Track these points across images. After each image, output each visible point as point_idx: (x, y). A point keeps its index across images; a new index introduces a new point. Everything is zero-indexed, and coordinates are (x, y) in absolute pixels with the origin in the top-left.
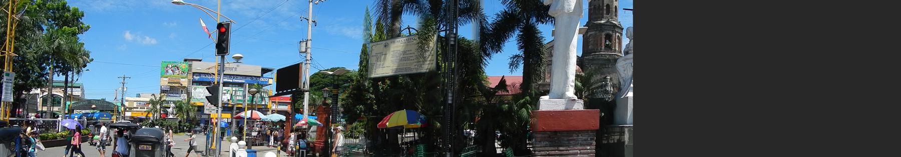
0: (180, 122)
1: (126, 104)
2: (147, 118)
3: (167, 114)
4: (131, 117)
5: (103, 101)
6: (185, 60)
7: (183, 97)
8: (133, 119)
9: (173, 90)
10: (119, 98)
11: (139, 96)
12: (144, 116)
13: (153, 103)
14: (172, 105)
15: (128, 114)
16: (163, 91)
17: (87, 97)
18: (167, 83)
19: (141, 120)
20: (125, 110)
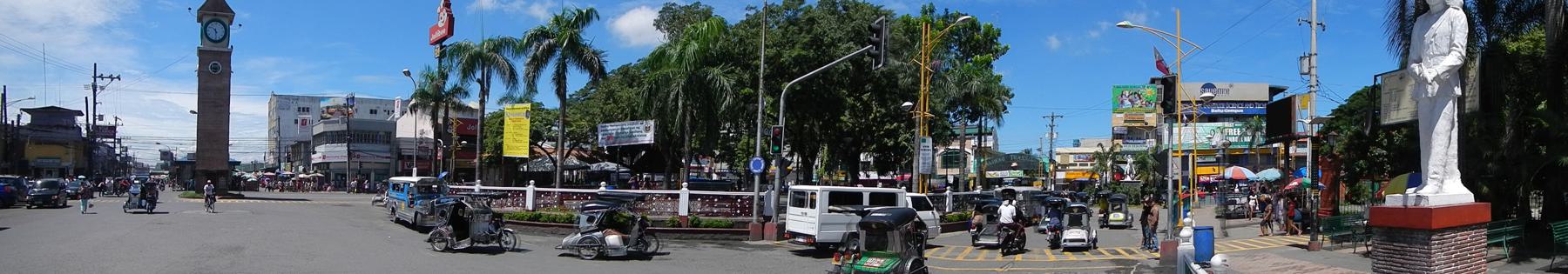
2: (1091, 182)
3: (1121, 173)
5: (1028, 152)
6: (1153, 81)
8: (1069, 184)
9: (1131, 133)
12: (1086, 178)
14: (1130, 160)
16: (1116, 136)
17: (1007, 148)
18: (1122, 123)
19: (1082, 185)
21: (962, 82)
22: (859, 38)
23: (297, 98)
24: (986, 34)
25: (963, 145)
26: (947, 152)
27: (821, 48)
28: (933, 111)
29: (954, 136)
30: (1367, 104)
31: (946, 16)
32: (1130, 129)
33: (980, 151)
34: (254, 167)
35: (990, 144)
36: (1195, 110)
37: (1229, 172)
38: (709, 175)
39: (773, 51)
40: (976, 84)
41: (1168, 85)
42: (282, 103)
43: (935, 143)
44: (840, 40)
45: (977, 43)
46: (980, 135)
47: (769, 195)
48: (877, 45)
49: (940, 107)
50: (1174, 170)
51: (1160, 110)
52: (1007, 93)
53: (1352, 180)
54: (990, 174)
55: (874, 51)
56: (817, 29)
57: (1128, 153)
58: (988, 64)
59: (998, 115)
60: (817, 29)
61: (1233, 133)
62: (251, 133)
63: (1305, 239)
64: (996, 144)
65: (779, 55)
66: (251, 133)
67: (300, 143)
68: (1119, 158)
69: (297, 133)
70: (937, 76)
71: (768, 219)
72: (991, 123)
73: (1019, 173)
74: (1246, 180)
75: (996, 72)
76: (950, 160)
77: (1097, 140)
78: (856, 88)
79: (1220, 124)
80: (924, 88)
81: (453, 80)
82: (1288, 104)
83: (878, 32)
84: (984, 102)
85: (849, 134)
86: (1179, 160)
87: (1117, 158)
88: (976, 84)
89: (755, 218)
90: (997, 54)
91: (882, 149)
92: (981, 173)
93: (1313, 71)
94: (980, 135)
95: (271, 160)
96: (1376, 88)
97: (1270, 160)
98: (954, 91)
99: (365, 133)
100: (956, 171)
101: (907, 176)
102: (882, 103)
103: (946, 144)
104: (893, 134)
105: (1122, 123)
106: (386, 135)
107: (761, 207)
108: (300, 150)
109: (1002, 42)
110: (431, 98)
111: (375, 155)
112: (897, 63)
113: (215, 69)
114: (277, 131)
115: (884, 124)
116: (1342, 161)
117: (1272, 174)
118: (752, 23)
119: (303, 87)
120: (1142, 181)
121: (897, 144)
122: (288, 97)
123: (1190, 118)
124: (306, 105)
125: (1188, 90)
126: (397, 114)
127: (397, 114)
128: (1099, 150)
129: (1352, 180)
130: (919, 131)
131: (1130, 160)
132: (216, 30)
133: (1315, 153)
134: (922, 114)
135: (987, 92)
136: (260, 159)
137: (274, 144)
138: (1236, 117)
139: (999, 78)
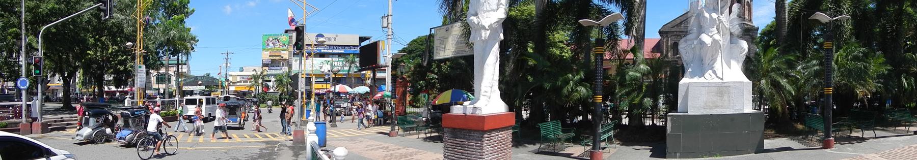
0: (281, 94)
1: (230, 79)
3: (268, 87)
5: (208, 75)
6: (286, 32)
7: (285, 69)
8: (237, 93)
9: (273, 63)
10: (223, 73)
11: (242, 70)
12: (246, 90)
13: (255, 78)
14: (273, 79)
15: (232, 88)
16: (265, 65)
17: (194, 73)
18: (268, 57)
19: (244, 94)
21: (166, 31)
25: (167, 70)
30: (423, 47)
32: (273, 61)
33: (179, 74)
36: (313, 50)
37: (339, 88)
40: (173, 33)
41: (300, 31)
43: (148, 67)
46: (178, 64)
50: (302, 86)
51: (291, 49)
52: (193, 39)
53: (416, 93)
54: (185, 88)
57: (271, 75)
58: (182, 21)
59: (187, 54)
61: (339, 64)
63: (387, 129)
68: (266, 78)
71: (35, 119)
73: (203, 87)
74: (347, 93)
76: (160, 79)
77: (253, 67)
79: (330, 59)
80: (140, 35)
82: (375, 46)
84: (180, 45)
86: (304, 80)
87: (265, 79)
88: (173, 33)
89: (24, 119)
90: (187, 14)
91: (117, 72)
92: (179, 88)
93: (390, 26)
94: (178, 64)
96: (431, 36)
97: (361, 81)
102: (115, 43)
103: (157, 69)
105: (268, 57)
109: (190, 7)
112: (123, 17)
116: (408, 82)
117: (363, 89)
120: (280, 92)
121: (126, 69)
123: (309, 54)
125: (310, 38)
128: (254, 73)
129: (416, 93)
130: (137, 60)
131: (273, 79)
133: (394, 78)
134: (139, 51)
138: (340, 55)
139: (189, 30)
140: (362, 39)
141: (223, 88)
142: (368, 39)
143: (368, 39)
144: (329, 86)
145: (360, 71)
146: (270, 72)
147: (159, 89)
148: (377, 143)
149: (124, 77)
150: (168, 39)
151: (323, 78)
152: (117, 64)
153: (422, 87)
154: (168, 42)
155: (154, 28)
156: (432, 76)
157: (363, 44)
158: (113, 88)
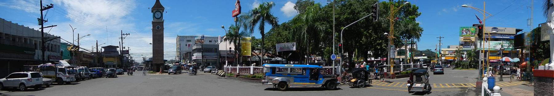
1: (442, 52)
3: (462, 58)
4: (445, 60)
6: (474, 25)
7: (473, 47)
11: (449, 47)
14: (465, 53)
15: (443, 58)
18: (463, 40)
20: (442, 56)
22: (367, 10)
23: (186, 37)
24: (413, 9)
25: (406, 48)
26: (400, 50)
27: (354, 15)
28: (394, 36)
29: (403, 45)
31: (399, 2)
32: (466, 42)
33: (411, 50)
34: (172, 62)
35: (415, 47)
38: (314, 61)
39: (338, 16)
42: (181, 39)
44: (361, 11)
45: (411, 12)
47: (338, 67)
48: (375, 13)
49: (397, 34)
50: (482, 57)
51: (477, 36)
54: (415, 58)
55: (374, 15)
56: (352, 7)
57: (464, 51)
58: (414, 19)
59: (418, 38)
60: (352, 7)
62: (171, 50)
64: (417, 47)
65: (340, 18)
66: (171, 50)
67: (188, 52)
68: (461, 52)
69: (187, 49)
70: (396, 24)
71: (338, 75)
72: (415, 40)
73: (426, 57)
75: (417, 22)
76: (401, 53)
78: (367, 28)
80: (392, 28)
81: (241, 30)
83: (376, 8)
84: (414, 33)
85: (364, 45)
86: (483, 54)
88: (410, 26)
90: (417, 15)
95: (177, 59)
98: (403, 29)
99: (209, 49)
100: (404, 57)
101: (385, 59)
104: (380, 44)
105: (463, 40)
106: (215, 49)
107: (335, 71)
108: (188, 55)
109: (419, 11)
110: (233, 36)
111: (212, 57)
113: (158, 28)
114: (180, 49)
115: (377, 41)
118: (330, 6)
119: (189, 33)
120: (469, 61)
122: (183, 37)
123: (488, 39)
124: (188, 39)
126: (219, 42)
127: (219, 42)
130: (390, 43)
131: (465, 53)
132: (158, 15)
135: (414, 29)
136: (174, 59)
137: (178, 53)
140: (517, 31)
141: (438, 58)
142: (521, 30)
143: (521, 30)
144: (500, 58)
145: (515, 49)
146: (464, 49)
147: (399, 59)
148: (521, 89)
149: (381, 53)
150: (407, 30)
151: (494, 53)
152: (376, 45)
153: (534, 57)
154: (407, 31)
155: (400, 25)
156: (540, 50)
157: (518, 33)
158: (373, 59)
